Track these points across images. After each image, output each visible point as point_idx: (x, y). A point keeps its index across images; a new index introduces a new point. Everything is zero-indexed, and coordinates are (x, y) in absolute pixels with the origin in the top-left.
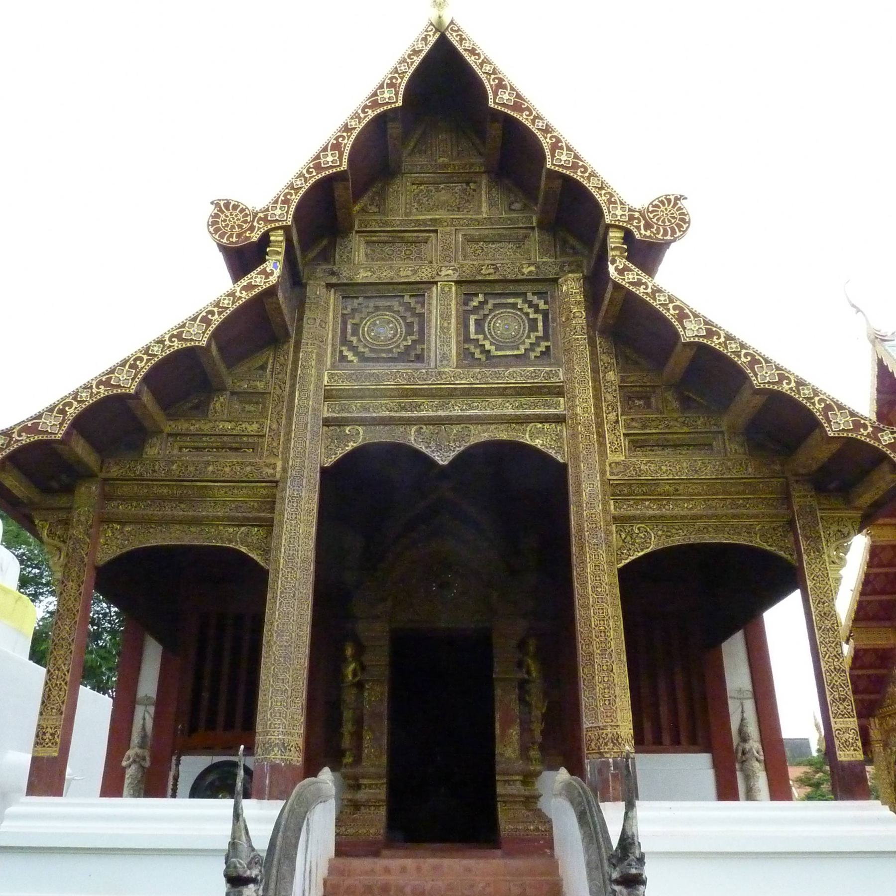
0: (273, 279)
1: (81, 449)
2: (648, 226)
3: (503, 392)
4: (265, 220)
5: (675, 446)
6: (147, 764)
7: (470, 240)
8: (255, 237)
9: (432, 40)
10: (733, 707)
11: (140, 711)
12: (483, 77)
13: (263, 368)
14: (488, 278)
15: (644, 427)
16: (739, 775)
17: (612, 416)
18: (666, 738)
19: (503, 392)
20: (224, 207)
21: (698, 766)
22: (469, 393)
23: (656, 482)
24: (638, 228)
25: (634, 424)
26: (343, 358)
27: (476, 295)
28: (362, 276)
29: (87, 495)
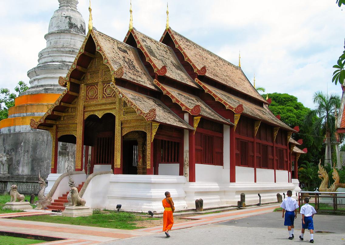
0: (66, 92)
1: (49, 122)
2: (117, 75)
3: (108, 104)
4: (65, 80)
5: (132, 113)
6: (90, 166)
7: (105, 72)
8: (64, 84)
9: (89, 35)
10: (185, 154)
11: (89, 156)
12: (95, 43)
13: (76, 102)
14: (106, 80)
15: (127, 109)
16: (184, 168)
17: (122, 108)
18: (173, 160)
19: (108, 104)
20: (61, 78)
21: (177, 166)
22: (103, 104)
23: (127, 120)
24: (115, 75)
25: (125, 109)
26: (87, 99)
27: (105, 84)
28: (89, 82)
29: (55, 127)
